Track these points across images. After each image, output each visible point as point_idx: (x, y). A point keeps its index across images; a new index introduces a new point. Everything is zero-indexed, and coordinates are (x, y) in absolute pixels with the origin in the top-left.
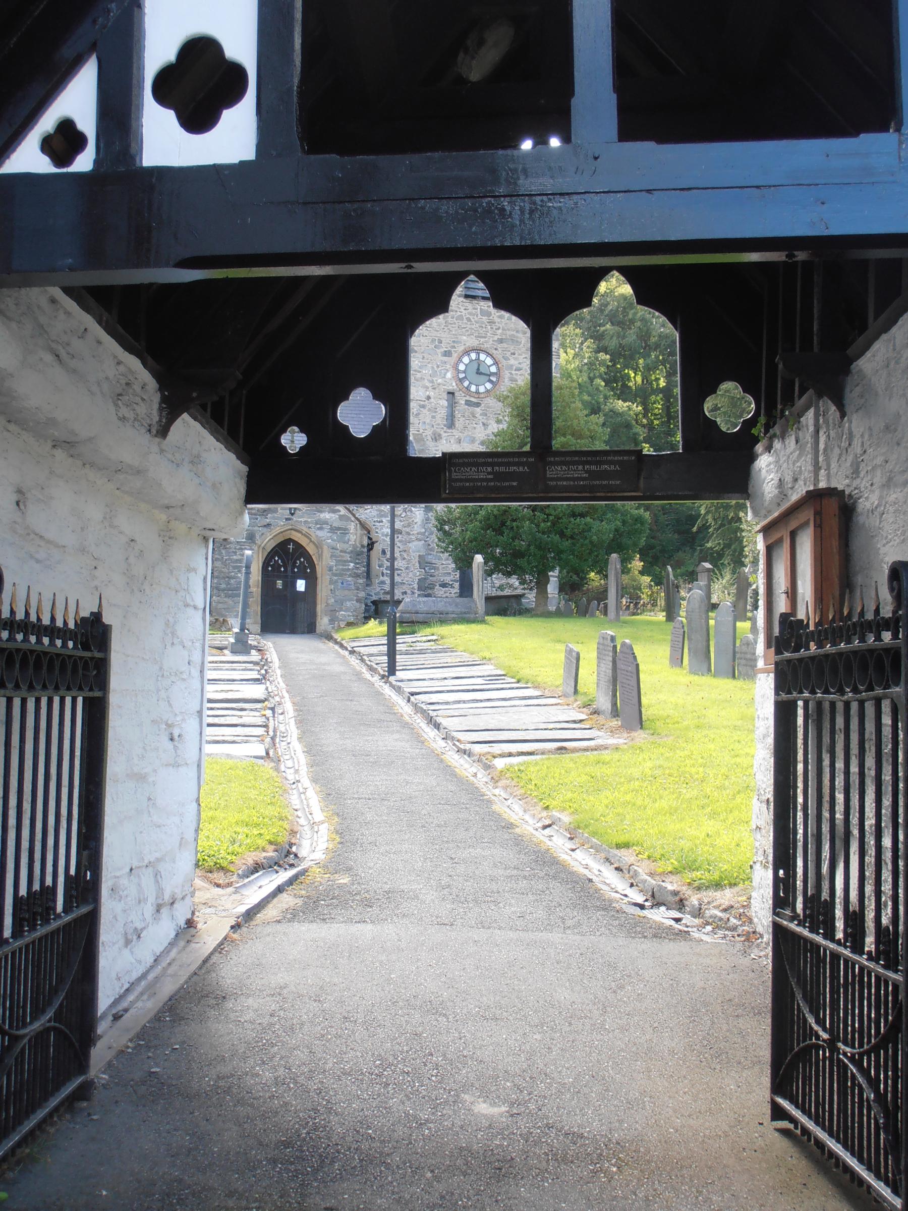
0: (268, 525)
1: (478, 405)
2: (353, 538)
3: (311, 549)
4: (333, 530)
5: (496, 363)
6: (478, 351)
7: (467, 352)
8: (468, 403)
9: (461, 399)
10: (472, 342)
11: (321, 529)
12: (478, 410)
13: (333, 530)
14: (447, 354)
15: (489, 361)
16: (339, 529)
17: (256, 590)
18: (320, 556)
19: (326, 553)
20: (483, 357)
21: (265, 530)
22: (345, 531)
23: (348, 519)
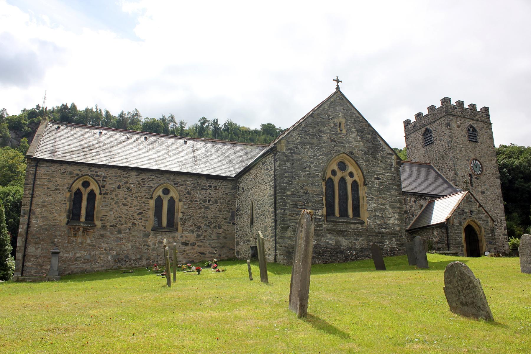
0: (465, 219)
1: (478, 179)
2: (490, 224)
3: (476, 229)
4: (484, 221)
5: (481, 164)
6: (476, 160)
7: (473, 160)
8: (476, 178)
9: (474, 177)
10: (473, 156)
11: (480, 220)
12: (478, 181)
13: (484, 221)
14: (467, 160)
15: (479, 164)
16: (485, 220)
17: (464, 244)
18: (481, 232)
19: (483, 230)
20: (477, 162)
21: (464, 221)
22: (487, 221)
23: (487, 217)
